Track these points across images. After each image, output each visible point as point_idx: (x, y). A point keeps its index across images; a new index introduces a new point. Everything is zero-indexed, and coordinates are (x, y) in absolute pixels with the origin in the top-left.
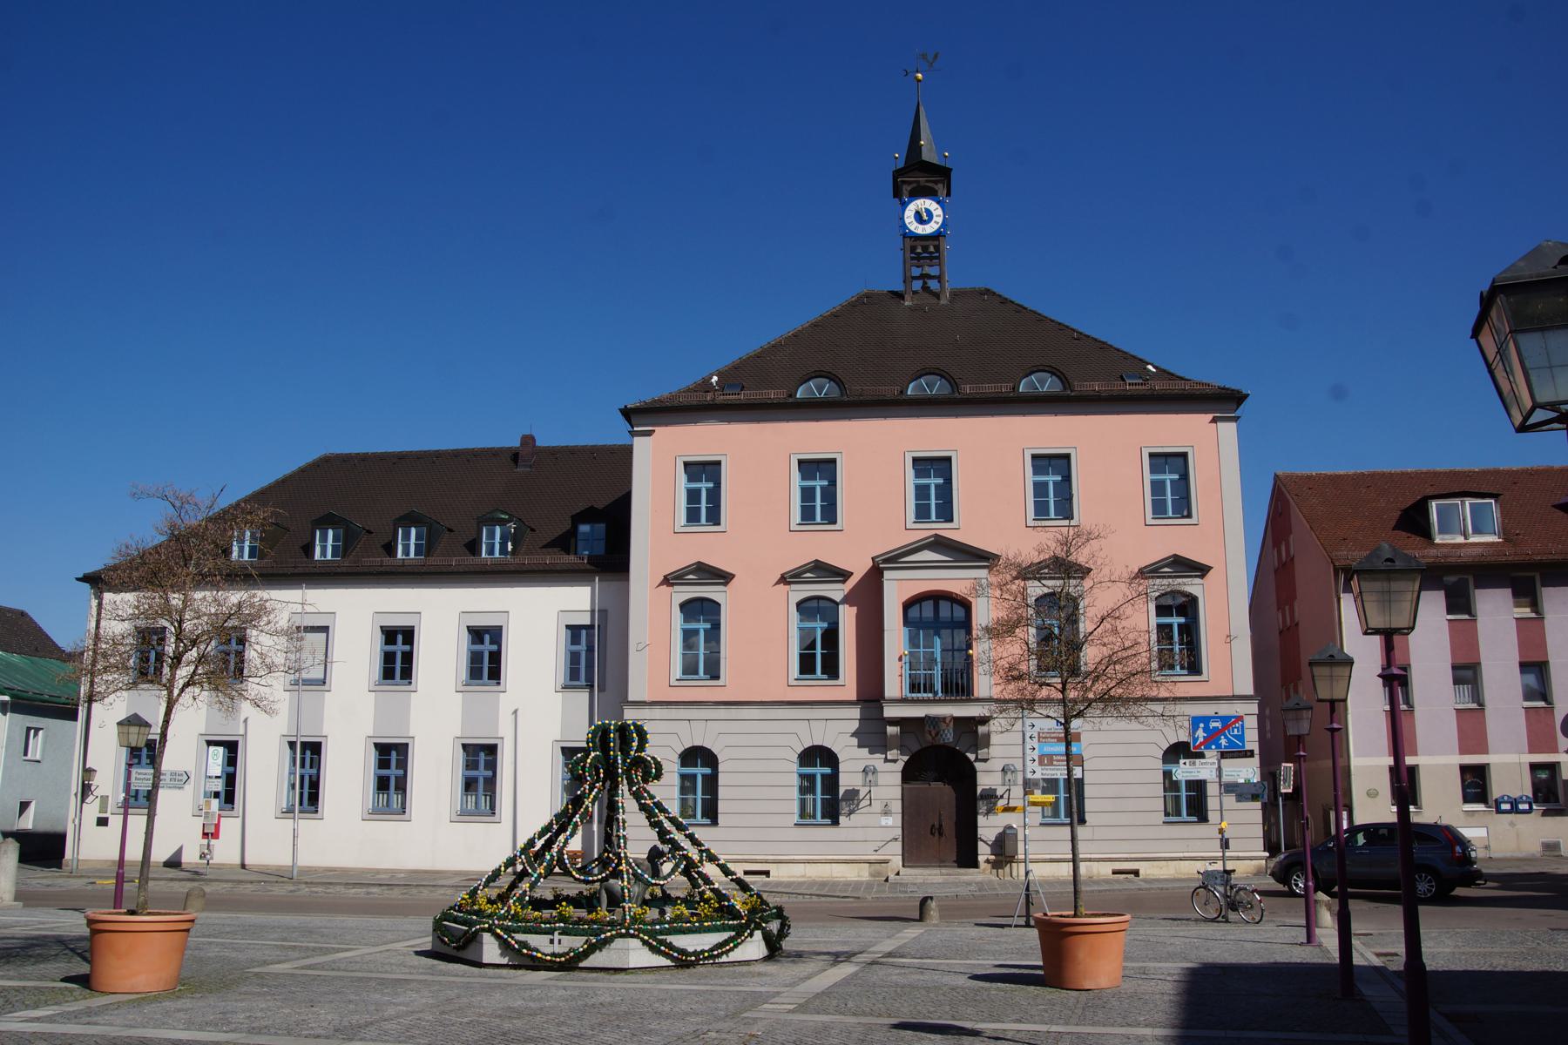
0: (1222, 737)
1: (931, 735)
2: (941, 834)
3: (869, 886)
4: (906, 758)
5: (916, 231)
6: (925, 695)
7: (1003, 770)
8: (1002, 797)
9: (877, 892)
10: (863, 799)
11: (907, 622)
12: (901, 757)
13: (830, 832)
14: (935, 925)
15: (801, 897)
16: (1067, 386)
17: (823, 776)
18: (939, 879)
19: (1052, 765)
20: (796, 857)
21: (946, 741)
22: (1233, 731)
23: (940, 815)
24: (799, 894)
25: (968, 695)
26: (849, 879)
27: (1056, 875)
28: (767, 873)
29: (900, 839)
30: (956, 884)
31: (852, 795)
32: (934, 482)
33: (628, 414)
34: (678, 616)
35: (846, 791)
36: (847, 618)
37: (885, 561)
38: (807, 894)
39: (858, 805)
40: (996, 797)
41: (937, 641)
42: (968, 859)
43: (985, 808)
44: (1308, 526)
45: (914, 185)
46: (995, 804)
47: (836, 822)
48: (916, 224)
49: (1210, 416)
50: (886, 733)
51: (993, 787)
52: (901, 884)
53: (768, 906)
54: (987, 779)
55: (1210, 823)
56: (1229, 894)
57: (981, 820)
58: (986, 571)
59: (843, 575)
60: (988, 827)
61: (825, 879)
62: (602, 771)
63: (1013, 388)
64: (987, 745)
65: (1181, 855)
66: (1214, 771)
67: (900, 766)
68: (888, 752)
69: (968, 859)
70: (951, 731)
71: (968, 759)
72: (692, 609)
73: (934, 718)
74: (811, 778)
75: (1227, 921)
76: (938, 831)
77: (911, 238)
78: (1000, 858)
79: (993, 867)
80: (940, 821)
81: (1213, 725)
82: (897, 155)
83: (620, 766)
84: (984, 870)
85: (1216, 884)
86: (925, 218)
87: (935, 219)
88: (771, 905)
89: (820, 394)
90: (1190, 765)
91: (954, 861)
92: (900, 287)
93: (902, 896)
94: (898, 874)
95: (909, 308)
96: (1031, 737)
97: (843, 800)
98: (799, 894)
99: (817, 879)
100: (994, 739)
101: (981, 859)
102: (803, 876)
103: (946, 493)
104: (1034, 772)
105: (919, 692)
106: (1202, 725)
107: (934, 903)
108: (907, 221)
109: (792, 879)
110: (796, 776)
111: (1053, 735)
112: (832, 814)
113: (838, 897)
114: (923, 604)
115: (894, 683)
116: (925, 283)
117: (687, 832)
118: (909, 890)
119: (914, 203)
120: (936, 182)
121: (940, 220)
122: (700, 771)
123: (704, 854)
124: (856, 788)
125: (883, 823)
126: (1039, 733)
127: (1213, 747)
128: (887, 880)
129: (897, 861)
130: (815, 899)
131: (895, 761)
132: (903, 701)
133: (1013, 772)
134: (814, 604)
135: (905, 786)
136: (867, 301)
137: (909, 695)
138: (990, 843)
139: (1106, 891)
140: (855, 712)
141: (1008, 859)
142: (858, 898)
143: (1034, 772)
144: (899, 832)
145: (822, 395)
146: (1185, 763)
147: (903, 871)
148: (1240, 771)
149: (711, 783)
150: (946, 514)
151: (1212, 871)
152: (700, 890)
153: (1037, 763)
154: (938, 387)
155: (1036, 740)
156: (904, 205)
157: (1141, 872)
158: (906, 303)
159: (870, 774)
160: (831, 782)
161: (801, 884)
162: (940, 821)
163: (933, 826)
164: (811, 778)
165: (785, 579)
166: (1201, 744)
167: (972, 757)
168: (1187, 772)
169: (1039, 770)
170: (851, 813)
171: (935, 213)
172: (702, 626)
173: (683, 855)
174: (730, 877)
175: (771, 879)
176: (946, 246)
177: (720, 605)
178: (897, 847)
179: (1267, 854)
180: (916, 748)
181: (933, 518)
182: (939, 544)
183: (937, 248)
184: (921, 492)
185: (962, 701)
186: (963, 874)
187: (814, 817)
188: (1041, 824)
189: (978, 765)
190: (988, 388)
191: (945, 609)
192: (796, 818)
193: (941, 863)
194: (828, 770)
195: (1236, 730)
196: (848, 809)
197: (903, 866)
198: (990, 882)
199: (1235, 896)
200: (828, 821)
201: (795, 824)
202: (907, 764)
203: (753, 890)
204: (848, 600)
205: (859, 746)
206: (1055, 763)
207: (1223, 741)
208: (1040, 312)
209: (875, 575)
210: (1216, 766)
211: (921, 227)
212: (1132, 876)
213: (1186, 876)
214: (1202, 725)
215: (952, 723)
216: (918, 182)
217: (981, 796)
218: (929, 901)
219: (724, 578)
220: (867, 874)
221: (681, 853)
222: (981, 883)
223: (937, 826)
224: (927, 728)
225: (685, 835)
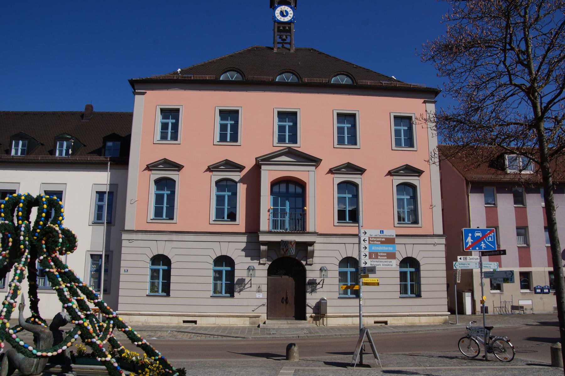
0: (482, 242)
1: (283, 250)
2: (287, 303)
3: (250, 330)
4: (270, 263)
5: (280, 20)
6: (281, 231)
7: (321, 270)
8: (319, 284)
9: (255, 334)
10: (247, 284)
11: (272, 193)
12: (267, 262)
13: (230, 301)
14: (298, 364)
15: (212, 337)
16: (355, 82)
17: (226, 271)
18: (287, 326)
19: (377, 258)
20: (211, 314)
21: (291, 254)
22: (489, 239)
23: (287, 293)
24: (211, 335)
25: (304, 230)
26: (238, 326)
27: (346, 324)
28: (195, 322)
29: (266, 305)
30: (297, 329)
31: (242, 281)
32: (288, 124)
33: (133, 83)
34: (153, 187)
35: (238, 279)
36: (242, 189)
37: (262, 160)
38: (216, 335)
39: (244, 287)
40: (316, 283)
41: (288, 203)
42: (300, 315)
43: (310, 289)
44: (451, 165)
47: (232, 296)
48: (280, 17)
49: (423, 100)
50: (260, 249)
51: (315, 279)
52: (267, 329)
53: (172, 370)
54: (311, 275)
56: (487, 343)
57: (308, 295)
58: (314, 168)
59: (240, 168)
60: (312, 299)
61: (226, 326)
62: (11, 240)
63: (329, 81)
64: (312, 257)
65: (408, 314)
66: (478, 264)
67: (267, 266)
68: (261, 260)
69: (300, 315)
70: (294, 249)
71: (302, 264)
72: (162, 183)
73: (286, 242)
74: (220, 272)
75: (487, 360)
76: (285, 301)
77: (277, 22)
78: (318, 315)
79: (314, 320)
80: (286, 295)
83: (22, 233)
84: (309, 321)
85: (477, 335)
86: (285, 14)
87: (289, 15)
88: (174, 368)
89: (232, 78)
90: (464, 260)
91: (294, 317)
92: (272, 46)
93: (269, 336)
94: (265, 323)
95: (276, 53)
96: (364, 240)
97: (236, 284)
98: (211, 335)
99: (222, 326)
100: (316, 254)
101: (308, 315)
102: (215, 324)
103: (294, 130)
104: (366, 263)
105: (278, 229)
106: (470, 235)
107: (296, 348)
108: (276, 15)
109: (208, 325)
110: (212, 271)
111: (378, 239)
112: (230, 292)
113: (233, 337)
114: (281, 185)
115: (265, 223)
116: (283, 45)
117: (96, 301)
118: (272, 333)
119: (280, 7)
121: (292, 16)
122: (161, 268)
123: (112, 322)
124: (244, 278)
125: (257, 297)
126: (369, 238)
127: (477, 248)
128: (259, 326)
129: (264, 316)
130: (220, 338)
131: (264, 264)
132: (270, 232)
133: (325, 271)
134: (224, 183)
135: (269, 277)
137: (273, 230)
138: (313, 307)
139: (376, 333)
140: (244, 239)
141: (322, 316)
142: (244, 338)
143: (366, 263)
144: (266, 301)
145: (233, 79)
146: (460, 259)
147: (267, 322)
148: (491, 264)
149: (167, 275)
150: (293, 139)
151: (475, 328)
152: (119, 349)
153: (368, 257)
154: (290, 78)
155: (367, 242)
156: (275, 9)
157: (388, 322)
158: (274, 51)
159: (251, 271)
160: (231, 275)
161: (213, 328)
162: (286, 295)
163: (283, 298)
164: (220, 272)
165: (210, 169)
166: (470, 246)
168: (462, 264)
170: (240, 291)
171: (289, 13)
172: (166, 192)
173: (79, 324)
174: (136, 343)
175: (197, 325)
176: (293, 26)
177: (175, 181)
178: (264, 309)
179: (449, 313)
180: (275, 257)
181: (287, 141)
182: (290, 152)
183: (290, 28)
184: (281, 129)
185: (300, 233)
186: (300, 324)
187: (221, 293)
188: (338, 298)
189: (307, 267)
190: (316, 80)
191: (292, 188)
192: (211, 293)
193: (286, 317)
194: (229, 269)
195: (490, 238)
196: (239, 289)
197: (267, 319)
198: (313, 328)
199: (493, 343)
200: (228, 295)
201: (211, 297)
202: (270, 266)
203: (158, 355)
204: (242, 181)
205: (246, 256)
206: (379, 257)
207: (483, 245)
208: (337, 57)
209: (257, 169)
210: (479, 261)
211: (283, 18)
212: (384, 324)
213: (411, 325)
214: (470, 235)
215: (295, 245)
217: (308, 283)
218: (293, 346)
219: (178, 167)
220: (248, 323)
221: (77, 322)
222: (309, 328)
223: (285, 298)
224: (282, 247)
225: (95, 303)
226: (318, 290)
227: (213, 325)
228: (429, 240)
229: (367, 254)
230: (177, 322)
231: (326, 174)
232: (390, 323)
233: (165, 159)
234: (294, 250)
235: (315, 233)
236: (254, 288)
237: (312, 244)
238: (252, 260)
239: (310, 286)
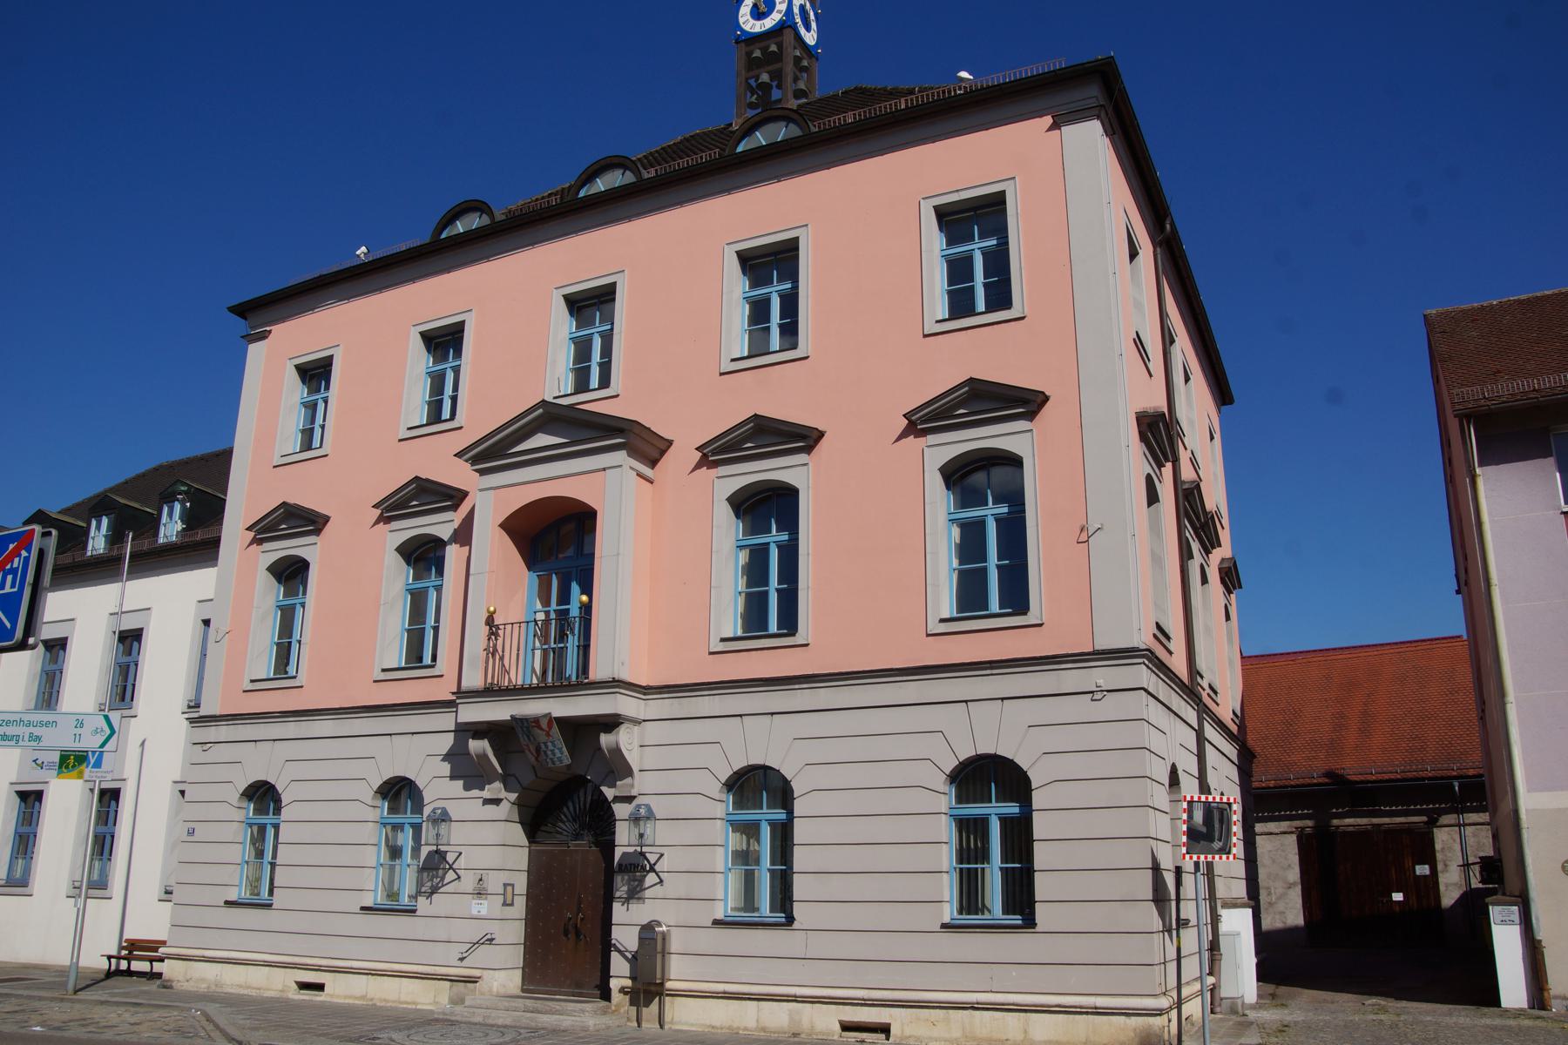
20: (309, 961)
27: (735, 1025)
28: (320, 987)
39: (443, 878)
43: (625, 888)
46: (642, 880)
55: (1037, 929)
61: (389, 1005)
84: (618, 1006)
91: (596, 986)
101: (614, 984)
102: (363, 997)
125: (475, 912)
129: (511, 980)
131: (497, 802)
157: (893, 1030)
167: (609, 793)
180: (528, 778)
196: (429, 884)
205: (453, 777)
217: (620, 865)
220: (447, 1001)
226: (648, 893)
227: (356, 1002)
228: (1071, 678)
230: (280, 987)
231: (693, 470)
232: (899, 1034)
233: (284, 504)
234: (560, 749)
235: (616, 684)
237: (611, 723)
238: (467, 788)
239: (626, 877)
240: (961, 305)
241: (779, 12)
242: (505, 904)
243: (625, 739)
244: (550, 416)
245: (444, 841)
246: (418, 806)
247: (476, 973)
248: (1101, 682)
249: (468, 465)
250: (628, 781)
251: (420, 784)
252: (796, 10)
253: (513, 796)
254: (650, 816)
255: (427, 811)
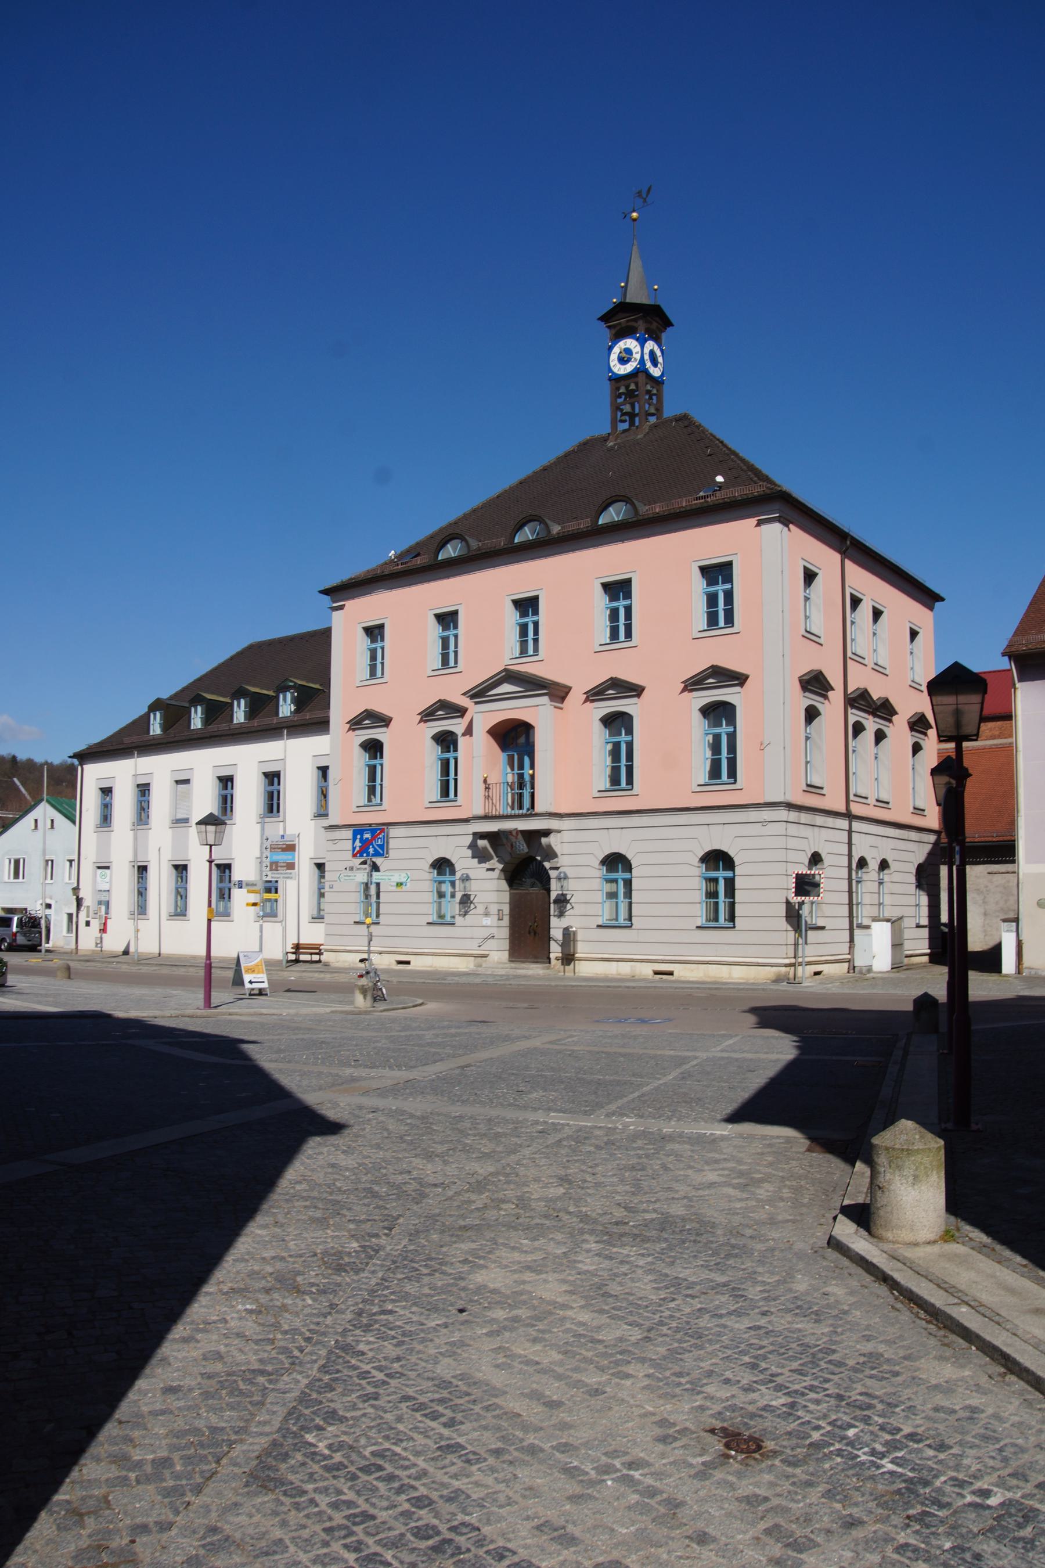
28: (408, 963)
45: (618, 328)
49: (753, 521)
57: (554, 921)
81: (367, 836)
82: (656, 287)
84: (554, 966)
101: (552, 956)
102: (431, 967)
106: (359, 836)
120: (635, 320)
131: (493, 870)
135: (512, 891)
136: (586, 446)
153: (268, 869)
166: (358, 852)
167: (547, 865)
169: (269, 874)
180: (507, 858)
213: (713, 980)
214: (359, 836)
216: (620, 323)
226: (566, 913)
228: (753, 815)
229: (268, 864)
236: (480, 909)
237: (547, 833)
238: (480, 862)
240: (712, 620)
241: (636, 353)
242: (499, 919)
243: (552, 840)
244: (509, 676)
245: (468, 889)
246: (453, 872)
247: (487, 953)
248: (766, 817)
249: (468, 699)
250: (556, 860)
251: (453, 861)
252: (647, 357)
253: (501, 866)
254: (566, 878)
255: (458, 875)
